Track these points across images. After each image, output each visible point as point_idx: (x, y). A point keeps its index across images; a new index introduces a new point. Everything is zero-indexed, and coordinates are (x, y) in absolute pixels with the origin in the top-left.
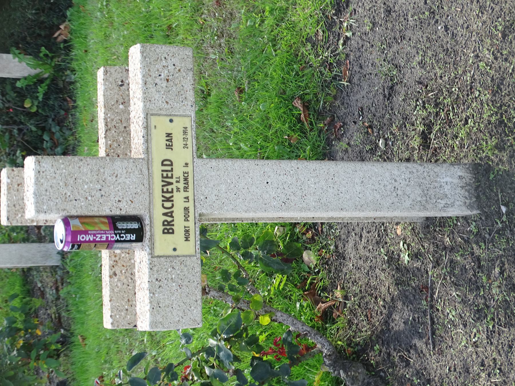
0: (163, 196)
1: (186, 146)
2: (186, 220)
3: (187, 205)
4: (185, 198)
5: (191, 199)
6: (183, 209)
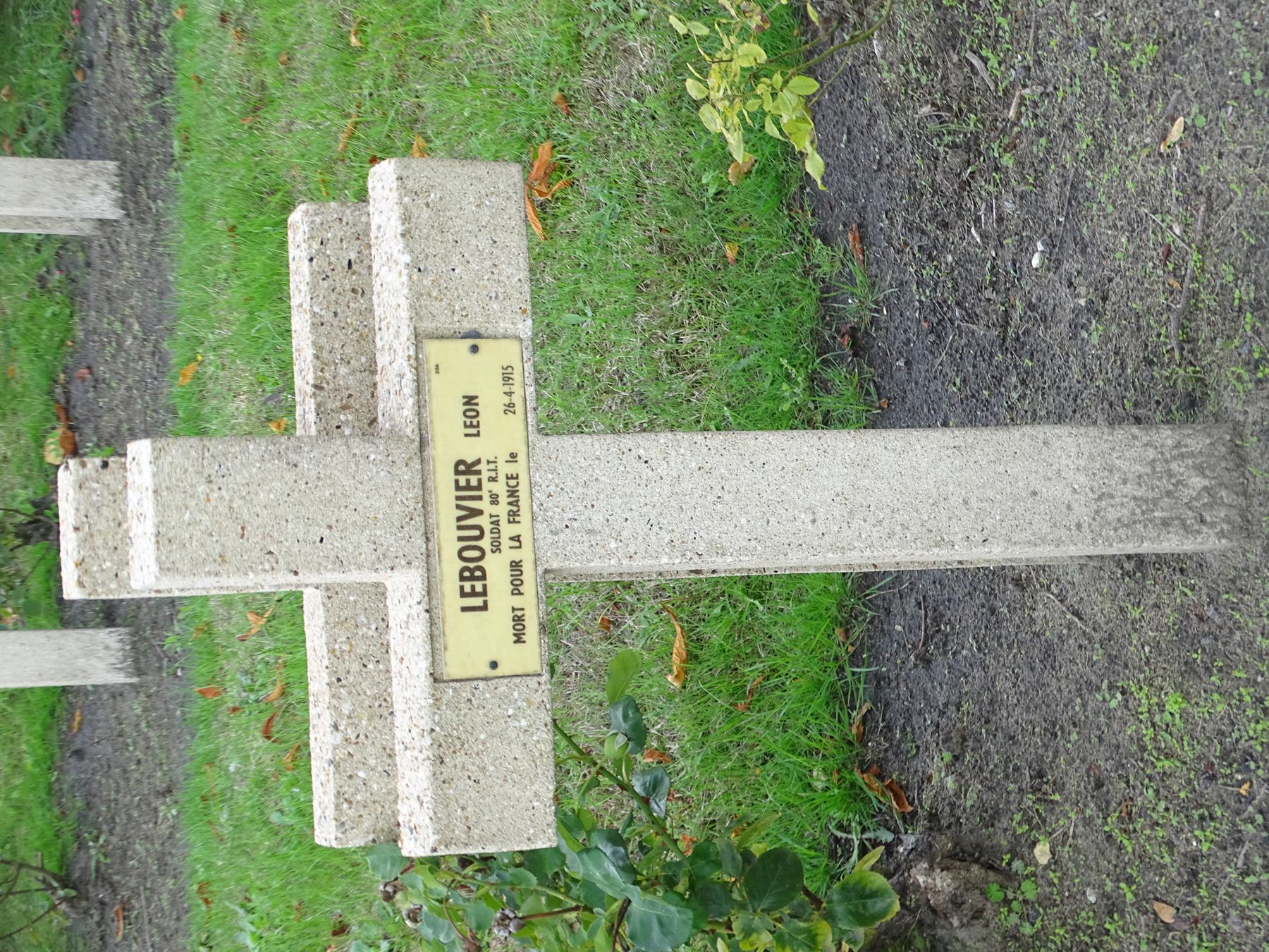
2: (517, 591)
3: (516, 555)
4: (512, 539)
5: (526, 540)
6: (509, 568)
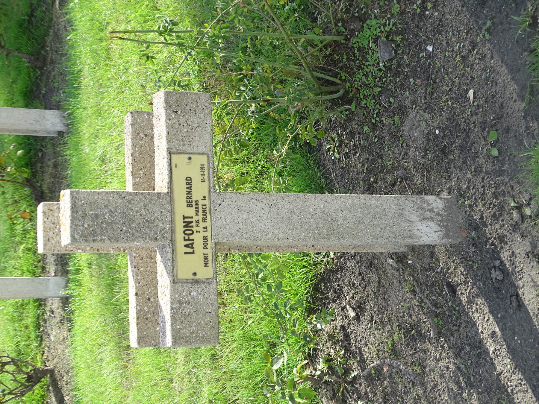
0: (184, 222)
1: (203, 180)
2: (205, 248)
3: (205, 234)
4: (204, 228)
5: (209, 228)
